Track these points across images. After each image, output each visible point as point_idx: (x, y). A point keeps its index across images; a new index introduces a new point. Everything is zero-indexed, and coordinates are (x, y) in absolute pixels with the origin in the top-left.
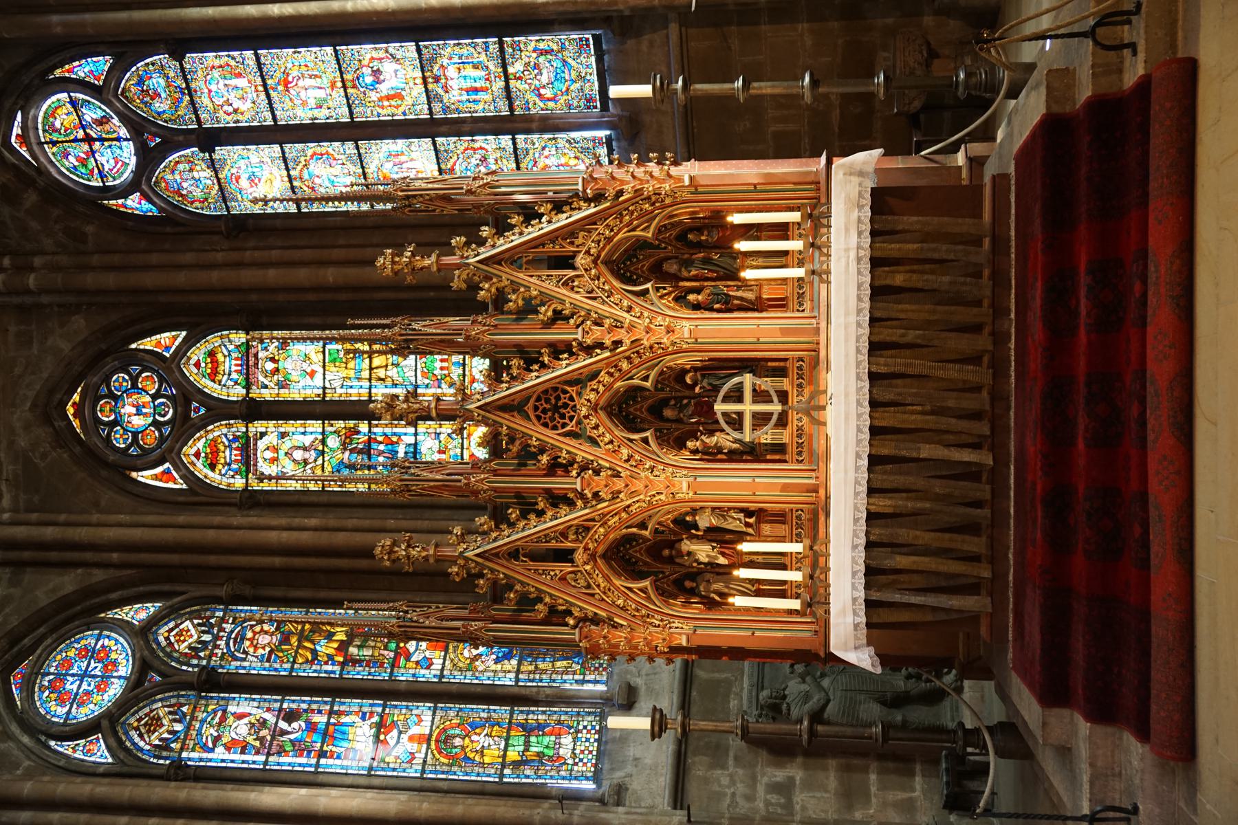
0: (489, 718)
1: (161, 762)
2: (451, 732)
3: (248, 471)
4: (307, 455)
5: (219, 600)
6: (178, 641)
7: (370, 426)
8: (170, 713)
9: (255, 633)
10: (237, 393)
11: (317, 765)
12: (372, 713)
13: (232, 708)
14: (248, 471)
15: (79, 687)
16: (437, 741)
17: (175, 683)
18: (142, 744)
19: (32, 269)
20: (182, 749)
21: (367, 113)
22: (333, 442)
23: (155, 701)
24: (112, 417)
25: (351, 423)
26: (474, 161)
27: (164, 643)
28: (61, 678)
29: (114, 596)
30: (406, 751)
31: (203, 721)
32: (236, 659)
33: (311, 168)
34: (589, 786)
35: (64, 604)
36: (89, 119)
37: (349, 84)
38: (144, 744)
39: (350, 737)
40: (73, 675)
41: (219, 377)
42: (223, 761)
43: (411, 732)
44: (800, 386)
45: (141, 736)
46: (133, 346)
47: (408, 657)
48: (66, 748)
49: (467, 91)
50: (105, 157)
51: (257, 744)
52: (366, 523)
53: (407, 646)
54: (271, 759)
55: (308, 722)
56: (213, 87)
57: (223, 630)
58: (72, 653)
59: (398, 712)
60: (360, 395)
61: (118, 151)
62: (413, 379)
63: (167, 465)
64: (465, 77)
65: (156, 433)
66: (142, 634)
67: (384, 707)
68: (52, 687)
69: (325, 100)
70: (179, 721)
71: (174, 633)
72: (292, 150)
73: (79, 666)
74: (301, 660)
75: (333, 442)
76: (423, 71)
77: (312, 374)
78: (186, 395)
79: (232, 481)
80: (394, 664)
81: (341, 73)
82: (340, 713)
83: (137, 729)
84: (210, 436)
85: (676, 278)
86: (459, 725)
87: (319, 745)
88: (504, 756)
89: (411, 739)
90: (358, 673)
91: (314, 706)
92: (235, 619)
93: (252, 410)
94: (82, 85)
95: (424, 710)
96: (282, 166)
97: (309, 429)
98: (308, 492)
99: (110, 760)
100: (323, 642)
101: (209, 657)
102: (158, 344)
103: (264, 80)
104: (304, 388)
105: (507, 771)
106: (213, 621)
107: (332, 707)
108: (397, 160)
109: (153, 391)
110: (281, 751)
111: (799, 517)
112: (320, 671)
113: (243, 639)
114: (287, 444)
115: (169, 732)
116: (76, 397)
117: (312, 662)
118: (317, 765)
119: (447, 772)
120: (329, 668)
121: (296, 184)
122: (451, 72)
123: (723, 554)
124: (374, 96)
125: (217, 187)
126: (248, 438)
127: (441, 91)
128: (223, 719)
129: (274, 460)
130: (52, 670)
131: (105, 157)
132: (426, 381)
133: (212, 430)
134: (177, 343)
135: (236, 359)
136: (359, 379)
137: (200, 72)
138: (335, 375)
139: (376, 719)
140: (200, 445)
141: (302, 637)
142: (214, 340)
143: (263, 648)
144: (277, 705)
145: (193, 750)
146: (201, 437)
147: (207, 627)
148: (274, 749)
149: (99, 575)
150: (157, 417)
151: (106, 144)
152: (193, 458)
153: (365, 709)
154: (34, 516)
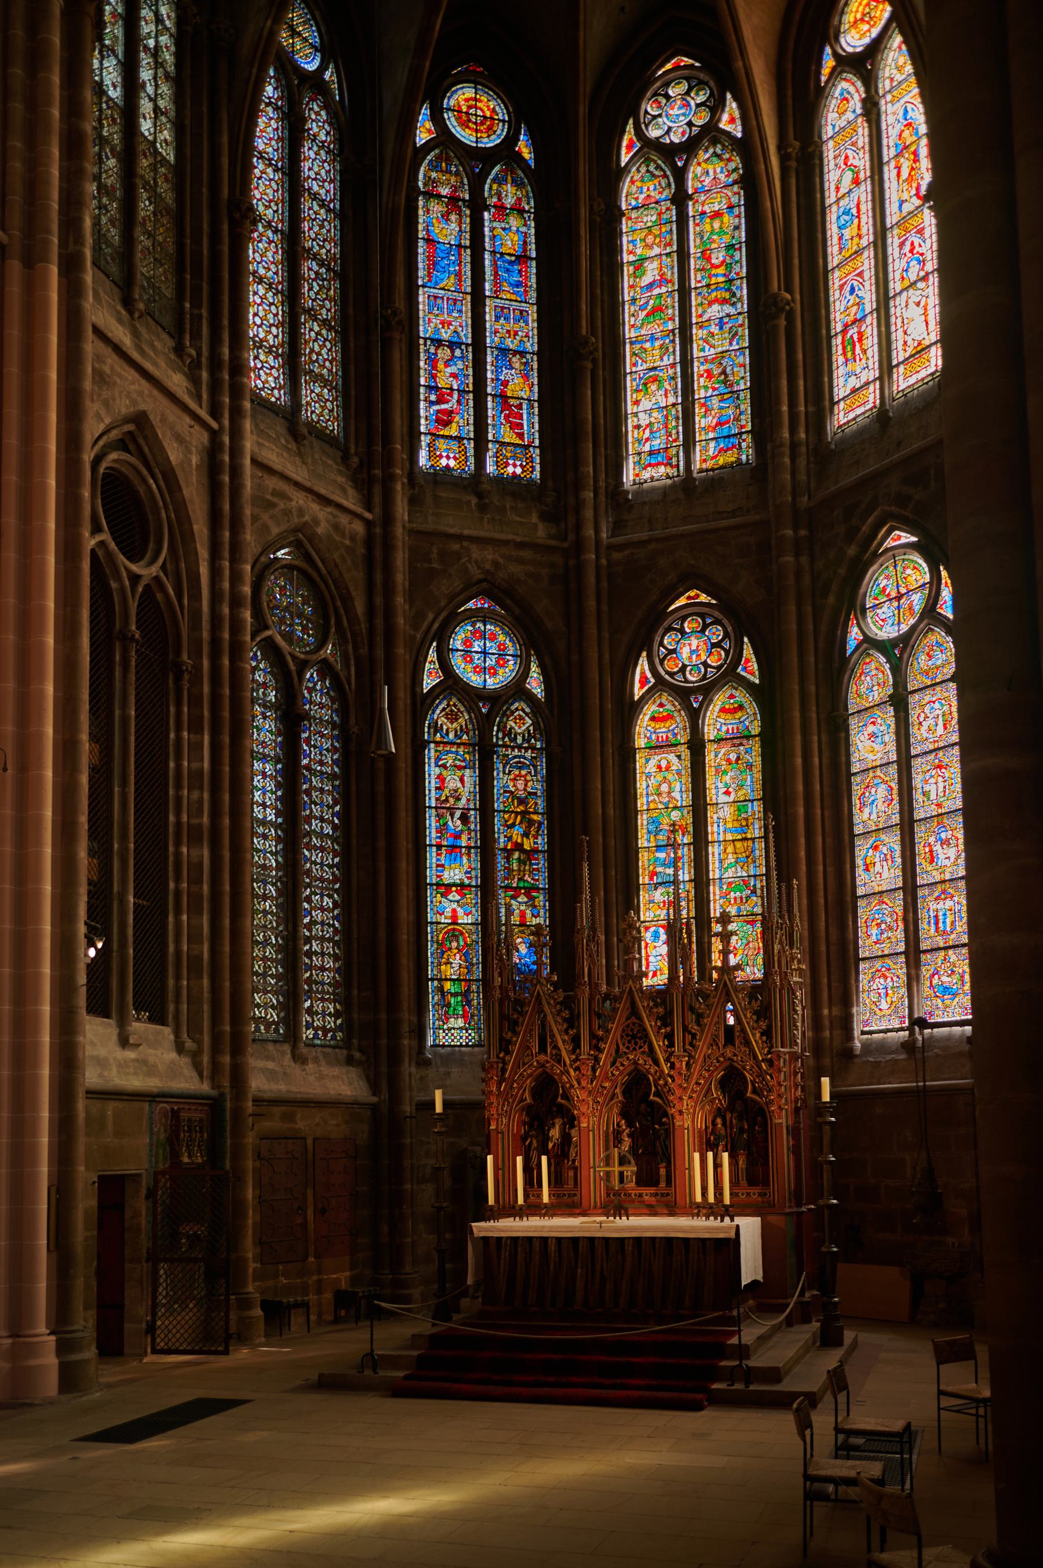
0: (472, 964)
1: (426, 730)
2: (461, 939)
3: (651, 748)
4: (664, 795)
5: (548, 743)
6: (515, 718)
7: (689, 844)
8: (461, 727)
9: (525, 776)
10: (710, 732)
11: (431, 845)
12: (469, 878)
13: (467, 772)
14: (651, 748)
15: (477, 652)
16: (454, 929)
17: (483, 725)
18: (438, 712)
19: (797, 554)
20: (437, 743)
21: (920, 832)
22: (675, 815)
23: (469, 713)
24: (688, 630)
25: (691, 829)
26: (889, 920)
27: (513, 708)
28: (482, 636)
29: (547, 660)
30: (445, 908)
31: (457, 753)
32: (504, 767)
33: (883, 786)
34: (430, 1041)
36: (913, 598)
37: (940, 818)
38: (438, 714)
39: (453, 866)
40: (485, 644)
41: (723, 715)
42: (429, 775)
43: (459, 909)
44: (656, 1195)
45: (444, 709)
46: (746, 640)
47: (514, 897)
48: (432, 655)
49: (936, 916)
50: (886, 611)
51: (443, 798)
52: (612, 854)
53: (522, 896)
54: (433, 810)
55: (462, 831)
56: (937, 705)
57: (526, 751)
58: (501, 638)
59: (472, 897)
60: (712, 833)
61: (891, 622)
62: (726, 876)
63: (653, 681)
64: (945, 915)
65: (676, 670)
66: (517, 689)
67: (476, 886)
68: (474, 633)
69: (929, 799)
70: (456, 735)
71: (521, 713)
72: (893, 769)
73: (492, 647)
74: (506, 816)
75: (675, 815)
76: (951, 880)
77: (727, 793)
78: (708, 690)
79: (642, 736)
80: (507, 888)
81: (947, 813)
82: (469, 855)
83: (448, 705)
84: (676, 714)
85: (731, 1108)
86: (466, 943)
87: (445, 843)
88: (446, 980)
89: (454, 911)
90: (500, 861)
91: (473, 834)
92: (535, 758)
95: (475, 916)
96: (884, 761)
97: (684, 796)
98: (636, 799)
99: (425, 691)
100: (521, 831)
101: (505, 746)
102: (748, 661)
103: (942, 748)
104: (717, 788)
105: (436, 983)
106: (533, 741)
107: (473, 847)
108: (889, 857)
109: (709, 662)
110: (439, 817)
111: (575, 1195)
112: (499, 833)
113: (520, 768)
115: (447, 730)
116: (703, 598)
117: (505, 825)
118: (431, 845)
119: (432, 941)
120: (502, 840)
121: (871, 771)
122: (949, 903)
123: (554, 1146)
124: (932, 840)
125: (868, 705)
126: (676, 745)
127: (936, 894)
128: (460, 768)
129: (659, 767)
130: (488, 627)
132: (725, 887)
133: (681, 715)
134: (749, 676)
135: (738, 728)
136: (725, 832)
137: (946, 694)
138: (727, 812)
139: (467, 882)
140: (669, 706)
142: (752, 707)
143: (514, 786)
144: (472, 806)
145: (436, 751)
146: (674, 705)
147: (528, 737)
148: (441, 811)
150: (689, 668)
151: (896, 612)
152: (658, 702)
153: (473, 873)
154: (605, 584)
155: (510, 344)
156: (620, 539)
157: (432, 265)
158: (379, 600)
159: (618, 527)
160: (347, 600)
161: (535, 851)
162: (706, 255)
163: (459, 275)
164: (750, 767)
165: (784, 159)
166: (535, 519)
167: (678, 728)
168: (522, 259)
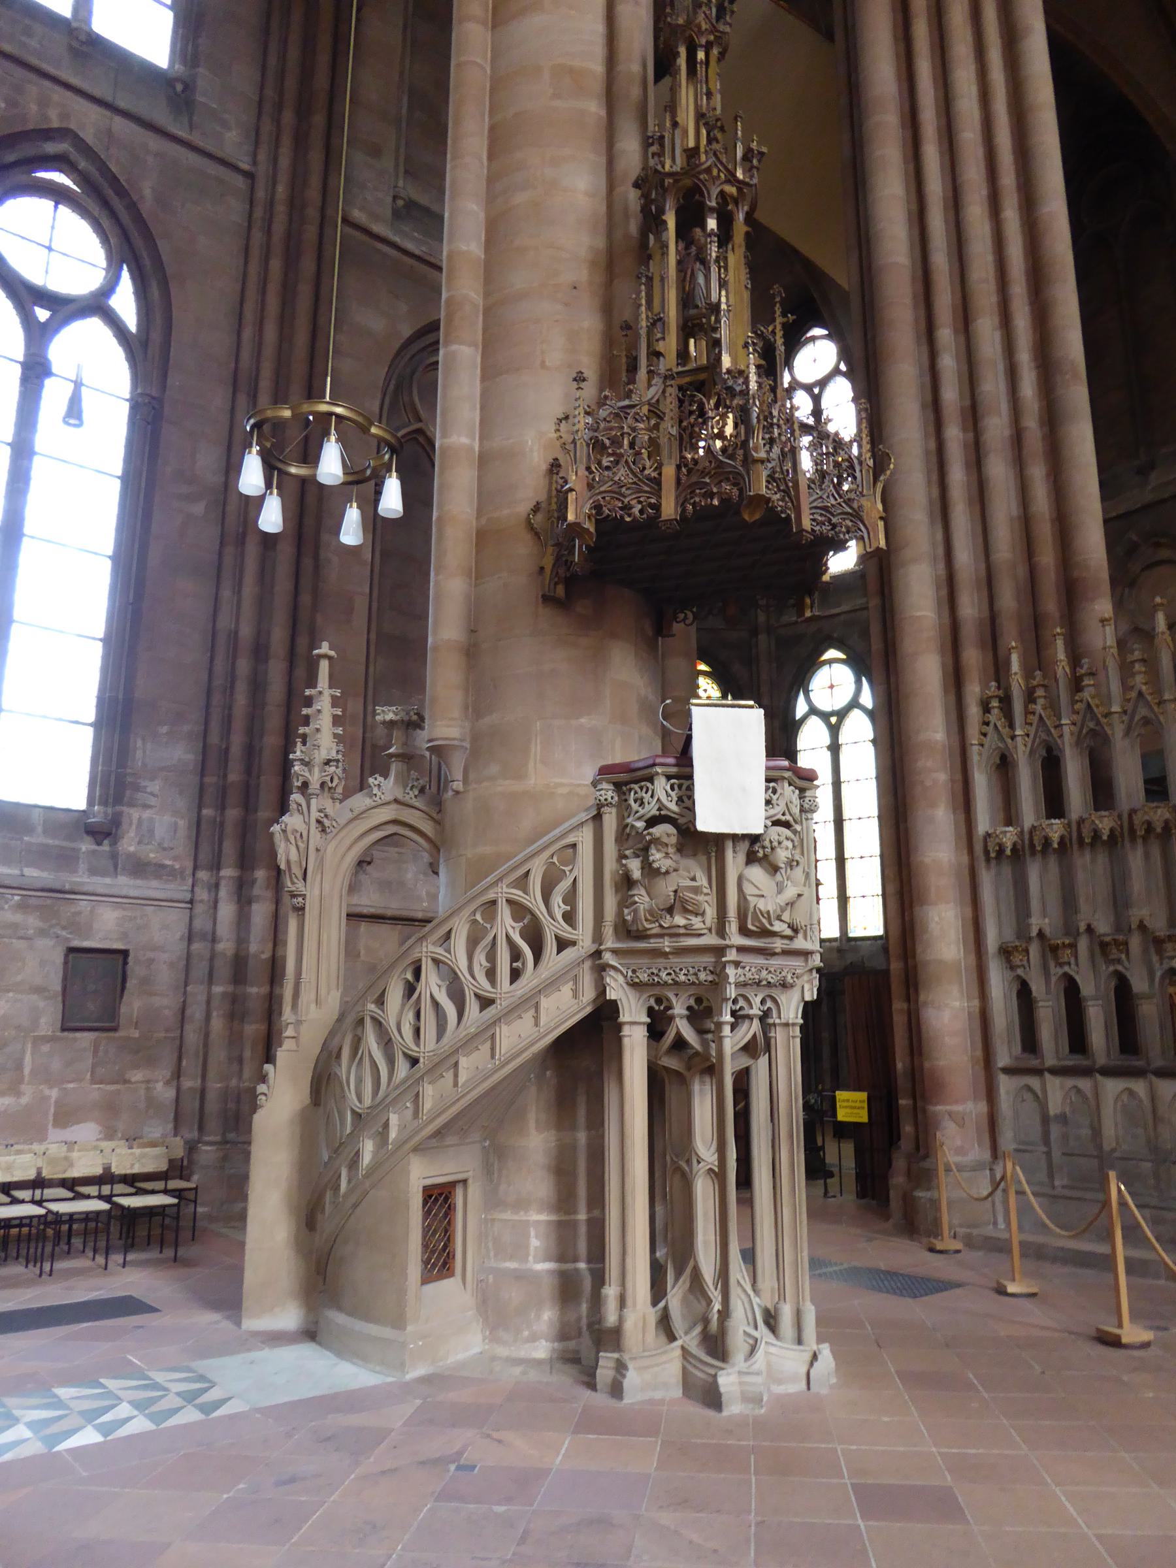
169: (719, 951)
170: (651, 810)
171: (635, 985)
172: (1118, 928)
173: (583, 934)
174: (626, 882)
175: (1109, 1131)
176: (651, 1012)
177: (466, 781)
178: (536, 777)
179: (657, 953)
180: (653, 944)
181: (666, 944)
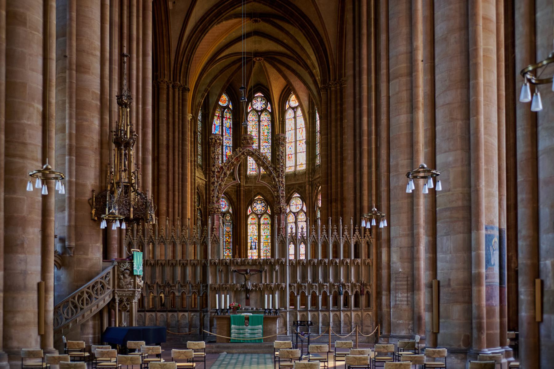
10: (262, 222)
22: (255, 237)
35: (232, 199)
66: (228, 212)
73: (224, 204)
78: (262, 215)
93: (259, 225)
94: (303, 207)
114: (255, 230)
116: (261, 197)
131: (294, 207)
141: (228, 235)
142: (269, 219)
149: (236, 204)
155: (228, 145)
156: (247, 185)
157: (215, 129)
158: (208, 196)
159: (246, 182)
160: (203, 196)
161: (230, 242)
162: (263, 133)
163: (219, 131)
164: (269, 229)
165: (279, 121)
166: (232, 179)
167: (256, 221)
168: (230, 128)
169: (134, 291)
170: (125, 268)
171: (118, 296)
172: (152, 283)
173: (111, 287)
174: (119, 279)
175: (147, 323)
176: (119, 300)
177: (74, 254)
178: (90, 256)
179: (125, 291)
180: (124, 289)
181: (126, 290)
